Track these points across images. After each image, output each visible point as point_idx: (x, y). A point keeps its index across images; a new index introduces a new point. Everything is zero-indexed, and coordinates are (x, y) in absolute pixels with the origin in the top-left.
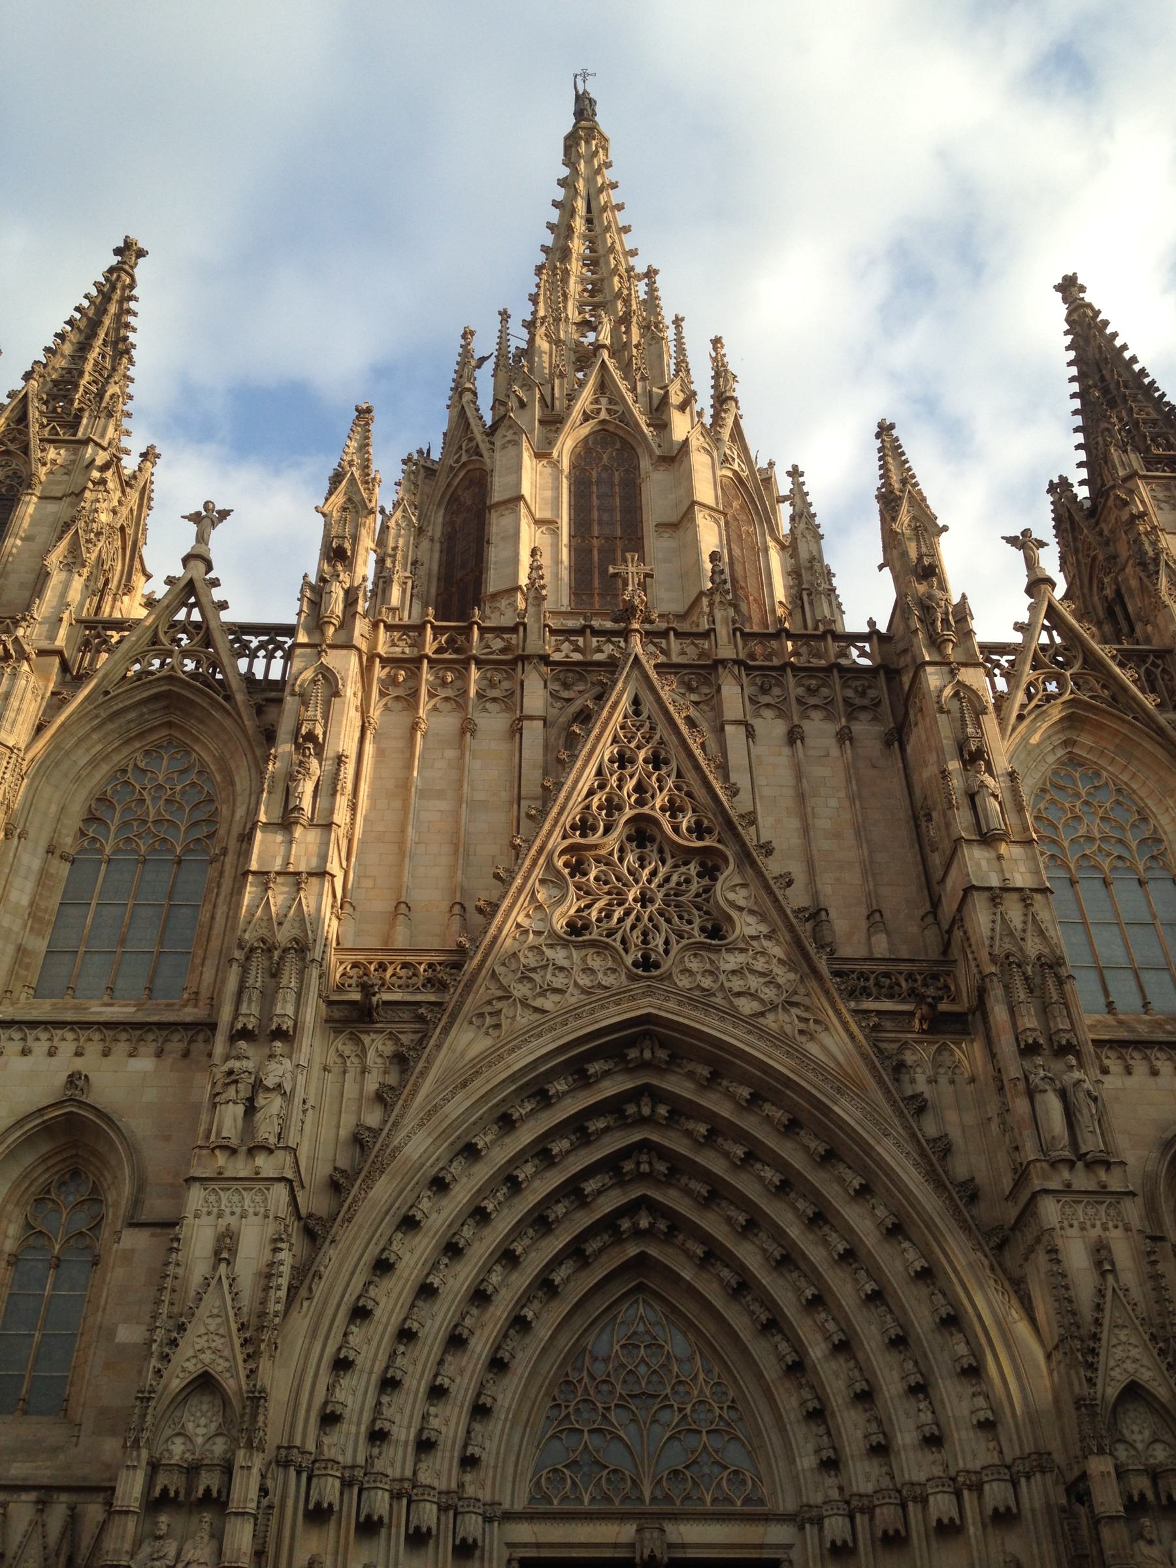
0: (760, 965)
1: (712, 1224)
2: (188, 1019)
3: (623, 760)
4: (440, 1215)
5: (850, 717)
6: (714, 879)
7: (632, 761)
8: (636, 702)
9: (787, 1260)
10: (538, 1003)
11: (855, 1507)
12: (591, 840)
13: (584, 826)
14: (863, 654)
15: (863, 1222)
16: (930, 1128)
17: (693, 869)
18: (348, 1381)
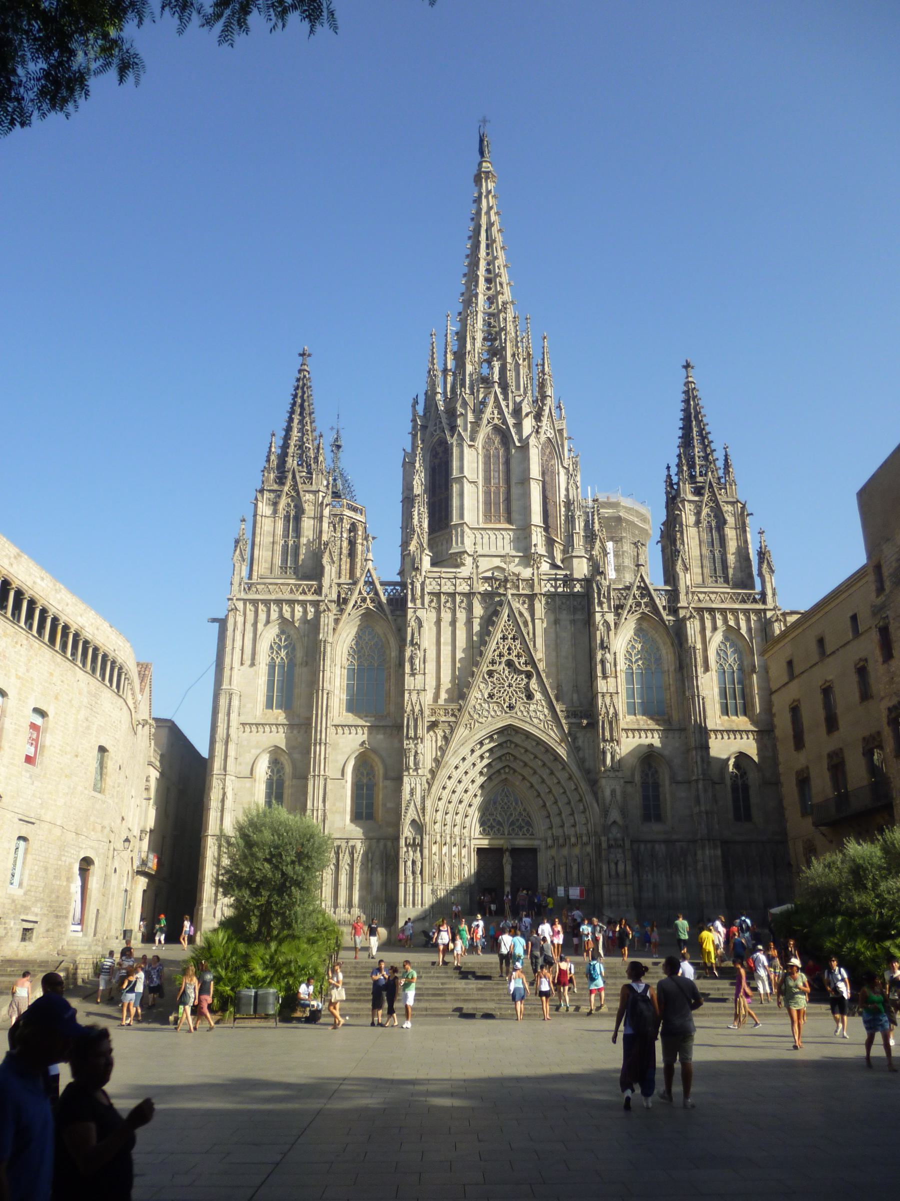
0: (540, 708)
1: (527, 772)
2: (390, 724)
3: (504, 638)
4: (456, 775)
5: (574, 613)
6: (530, 679)
7: (507, 639)
8: (508, 616)
9: (543, 781)
10: (480, 720)
11: (555, 839)
12: (495, 667)
13: (493, 663)
14: (581, 587)
15: (562, 776)
16: (581, 754)
17: (523, 676)
18: (439, 813)
